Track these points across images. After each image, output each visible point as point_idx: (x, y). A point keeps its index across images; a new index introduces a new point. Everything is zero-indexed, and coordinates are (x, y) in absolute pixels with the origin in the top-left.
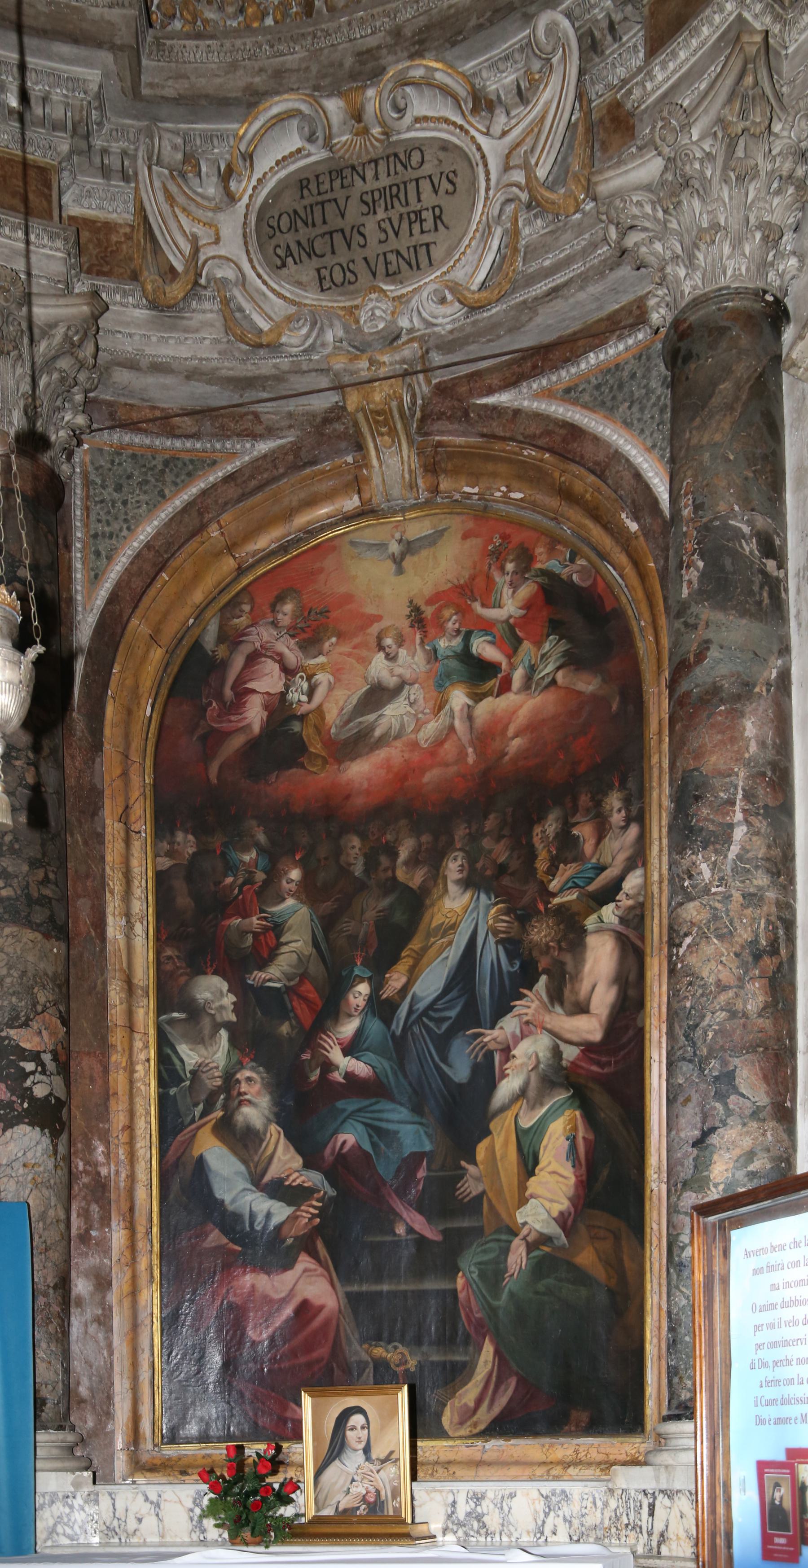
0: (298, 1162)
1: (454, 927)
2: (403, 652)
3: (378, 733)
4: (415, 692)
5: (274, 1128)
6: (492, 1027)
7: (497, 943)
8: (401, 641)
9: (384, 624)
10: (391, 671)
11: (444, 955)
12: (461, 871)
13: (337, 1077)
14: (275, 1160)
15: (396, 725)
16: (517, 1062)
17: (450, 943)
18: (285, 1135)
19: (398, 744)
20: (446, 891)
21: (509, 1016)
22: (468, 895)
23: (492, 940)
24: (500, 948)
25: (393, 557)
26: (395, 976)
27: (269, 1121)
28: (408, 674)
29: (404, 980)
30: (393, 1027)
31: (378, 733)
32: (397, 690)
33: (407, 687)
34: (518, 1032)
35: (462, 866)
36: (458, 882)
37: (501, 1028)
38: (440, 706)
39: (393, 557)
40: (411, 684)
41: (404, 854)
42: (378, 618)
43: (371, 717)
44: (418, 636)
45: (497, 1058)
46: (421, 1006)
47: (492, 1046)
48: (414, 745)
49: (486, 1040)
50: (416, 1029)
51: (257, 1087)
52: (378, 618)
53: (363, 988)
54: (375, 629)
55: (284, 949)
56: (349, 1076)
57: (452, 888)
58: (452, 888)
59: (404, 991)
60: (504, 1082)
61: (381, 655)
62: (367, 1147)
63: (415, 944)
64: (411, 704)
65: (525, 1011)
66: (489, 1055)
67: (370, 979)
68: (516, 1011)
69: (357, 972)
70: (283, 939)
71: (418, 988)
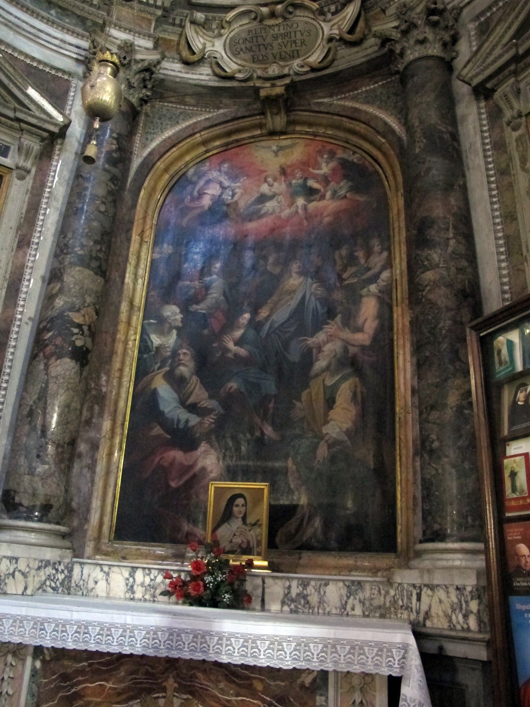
0: (205, 395)
1: (294, 292)
2: (276, 184)
3: (263, 212)
4: (280, 198)
5: (195, 378)
6: (312, 336)
7: (316, 299)
8: (275, 180)
9: (269, 173)
10: (270, 190)
11: (289, 303)
12: (299, 268)
13: (230, 355)
14: (194, 394)
15: (271, 210)
16: (325, 353)
17: (292, 298)
18: (201, 382)
19: (272, 217)
20: (291, 276)
21: (321, 332)
22: (302, 279)
23: (313, 299)
24: (317, 302)
25: (274, 152)
26: (264, 311)
27: (193, 374)
28: (277, 191)
29: (268, 313)
30: (261, 334)
31: (263, 212)
32: (272, 197)
33: (277, 196)
34: (325, 339)
35: (299, 266)
36: (297, 273)
37: (317, 337)
38: (292, 203)
39: (274, 152)
40: (279, 195)
41: (271, 260)
42: (265, 171)
43: (260, 206)
44: (283, 179)
45: (315, 351)
46: (276, 325)
47: (312, 345)
48: (279, 218)
49: (309, 342)
50: (273, 335)
51: (188, 358)
52: (265, 171)
53: (247, 316)
54: (264, 175)
55: (210, 296)
56: (236, 355)
57: (294, 275)
58: (294, 275)
59: (267, 318)
60: (317, 363)
61: (266, 184)
62: (243, 390)
63: (275, 298)
64: (278, 202)
65: (329, 330)
66: (310, 351)
67: (251, 313)
68: (324, 330)
69: (244, 308)
70: (209, 292)
71: (274, 317)
